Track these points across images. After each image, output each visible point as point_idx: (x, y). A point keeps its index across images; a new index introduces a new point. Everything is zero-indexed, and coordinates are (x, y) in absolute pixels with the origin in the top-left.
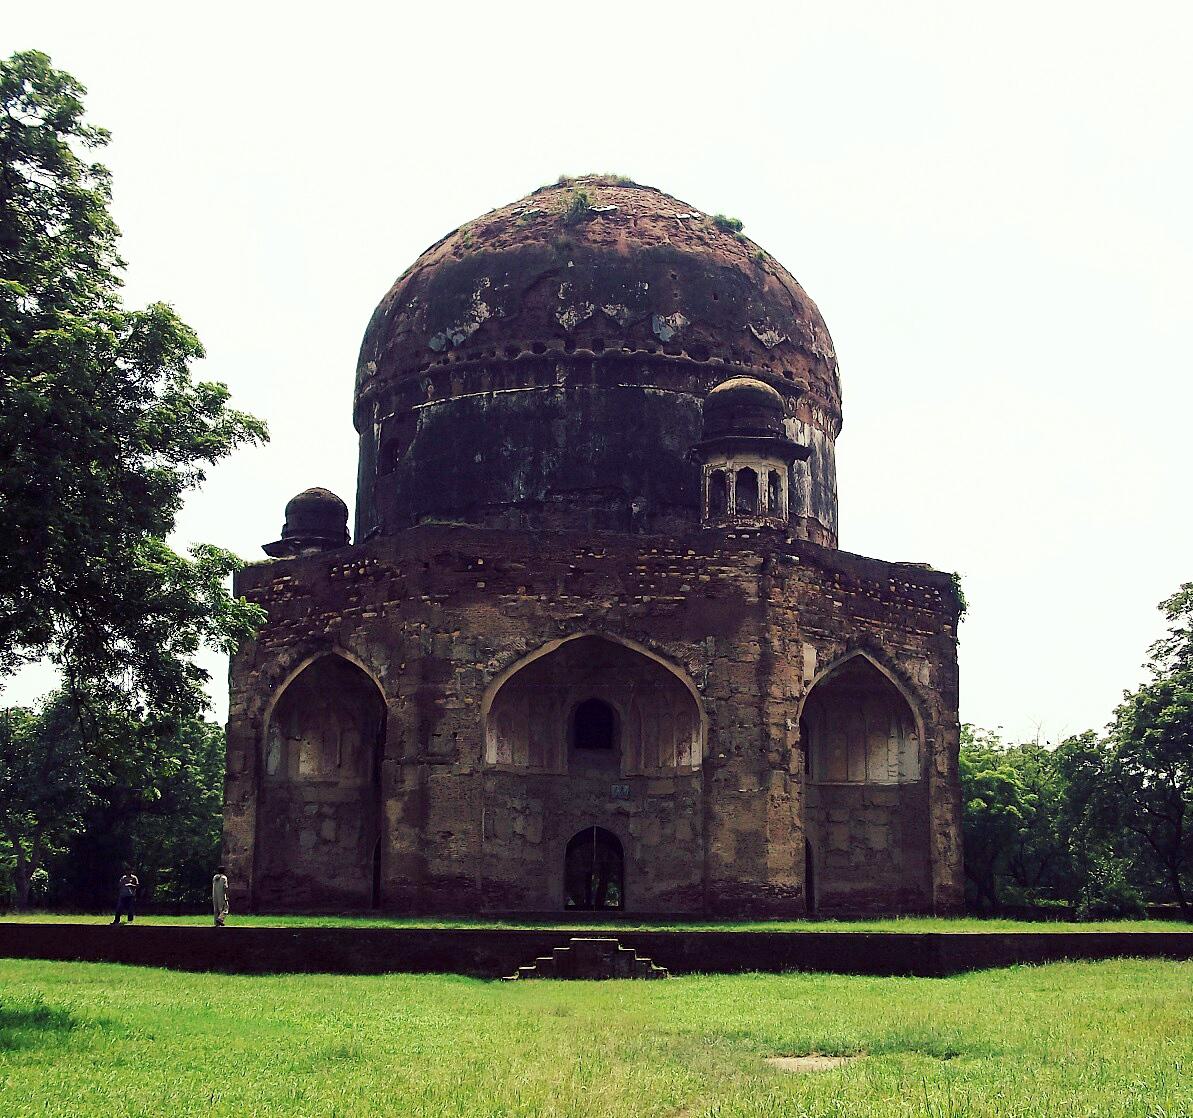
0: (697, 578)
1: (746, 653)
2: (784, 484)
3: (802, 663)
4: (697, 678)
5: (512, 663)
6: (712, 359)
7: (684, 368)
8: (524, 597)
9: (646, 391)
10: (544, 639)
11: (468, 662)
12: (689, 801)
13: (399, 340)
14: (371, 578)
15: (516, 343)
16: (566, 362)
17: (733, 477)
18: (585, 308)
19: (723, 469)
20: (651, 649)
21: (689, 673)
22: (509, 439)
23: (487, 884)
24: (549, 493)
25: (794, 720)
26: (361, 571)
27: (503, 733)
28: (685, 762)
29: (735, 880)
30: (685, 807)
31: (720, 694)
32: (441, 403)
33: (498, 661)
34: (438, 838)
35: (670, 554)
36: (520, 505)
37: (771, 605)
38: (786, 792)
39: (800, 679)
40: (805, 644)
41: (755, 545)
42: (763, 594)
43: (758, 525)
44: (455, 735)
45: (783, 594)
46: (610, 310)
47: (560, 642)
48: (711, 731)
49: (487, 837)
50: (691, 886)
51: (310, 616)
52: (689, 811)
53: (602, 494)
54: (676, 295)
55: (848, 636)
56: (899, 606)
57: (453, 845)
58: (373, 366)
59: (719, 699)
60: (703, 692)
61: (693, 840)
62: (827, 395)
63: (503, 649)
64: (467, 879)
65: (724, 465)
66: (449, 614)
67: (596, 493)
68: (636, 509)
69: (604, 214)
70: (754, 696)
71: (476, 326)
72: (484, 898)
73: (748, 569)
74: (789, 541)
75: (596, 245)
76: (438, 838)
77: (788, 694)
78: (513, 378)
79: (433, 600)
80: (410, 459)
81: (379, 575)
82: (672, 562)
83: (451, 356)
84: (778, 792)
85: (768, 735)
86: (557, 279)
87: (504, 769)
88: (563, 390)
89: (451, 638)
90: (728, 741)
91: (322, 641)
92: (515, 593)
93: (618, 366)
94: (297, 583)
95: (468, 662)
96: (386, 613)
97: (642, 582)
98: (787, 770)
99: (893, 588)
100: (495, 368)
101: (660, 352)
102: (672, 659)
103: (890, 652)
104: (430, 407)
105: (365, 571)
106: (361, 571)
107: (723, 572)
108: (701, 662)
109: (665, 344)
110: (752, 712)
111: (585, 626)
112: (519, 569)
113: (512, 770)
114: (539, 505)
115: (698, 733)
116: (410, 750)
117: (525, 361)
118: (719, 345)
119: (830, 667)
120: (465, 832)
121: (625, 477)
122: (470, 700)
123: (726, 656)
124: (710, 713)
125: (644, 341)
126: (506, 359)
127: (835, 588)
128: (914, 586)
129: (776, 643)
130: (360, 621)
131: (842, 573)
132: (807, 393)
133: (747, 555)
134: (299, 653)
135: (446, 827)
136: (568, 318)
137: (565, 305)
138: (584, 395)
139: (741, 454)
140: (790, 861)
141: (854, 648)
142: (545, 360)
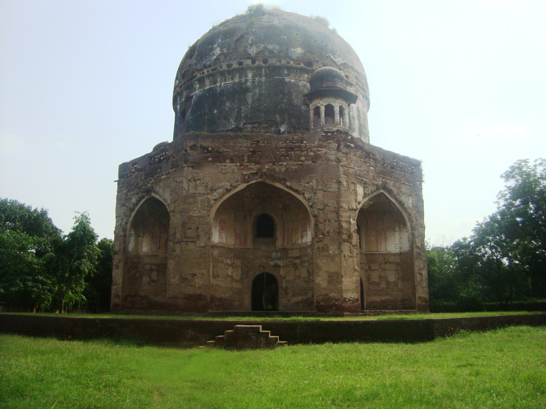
0: (308, 153)
1: (331, 187)
2: (346, 112)
3: (356, 194)
4: (308, 200)
5: (224, 194)
6: (314, 67)
7: (302, 71)
8: (229, 165)
9: (286, 80)
10: (238, 183)
11: (204, 194)
12: (306, 259)
13: (188, 68)
14: (165, 160)
15: (231, 62)
16: (251, 69)
17: (323, 109)
18: (259, 46)
19: (319, 105)
20: (287, 187)
21: (305, 198)
22: (228, 102)
23: (213, 298)
24: (245, 124)
25: (354, 220)
26: (162, 158)
27: (222, 229)
28: (304, 241)
29: (327, 295)
30: (304, 262)
31: (319, 207)
32: (201, 91)
33: (217, 194)
34: (190, 277)
35: (295, 143)
36: (232, 130)
37: (342, 166)
38: (351, 253)
39: (356, 201)
40: (358, 185)
41: (334, 138)
42: (339, 161)
43: (335, 129)
44: (198, 228)
45: (347, 161)
46: (270, 47)
47: (244, 185)
48: (316, 225)
49: (214, 277)
50: (308, 299)
51: (143, 181)
52: (307, 264)
53: (268, 124)
54: (298, 41)
55: (377, 183)
56: (398, 172)
57: (196, 280)
58: (177, 82)
59: (319, 209)
60: (311, 207)
61: (309, 277)
62: (363, 89)
63: (220, 188)
64: (202, 296)
65: (318, 103)
66: (196, 173)
67: (266, 123)
68: (282, 130)
69: (269, 14)
70: (335, 208)
71: (215, 57)
72: (213, 305)
73: (331, 149)
74: (349, 137)
75: (264, 23)
76: (190, 277)
77: (351, 207)
78: (230, 77)
79: (188, 167)
80: (189, 116)
81: (168, 158)
82: (296, 147)
83: (205, 71)
84: (347, 253)
85: (342, 227)
86: (248, 36)
88: (251, 80)
89: (196, 183)
90: (323, 229)
91: (148, 191)
92: (225, 162)
93: (275, 70)
94: (139, 167)
95: (204, 194)
96: (170, 175)
97: (283, 156)
98: (351, 243)
99: (395, 164)
100: (222, 74)
101: (292, 63)
102: (297, 191)
103: (395, 191)
104: (197, 92)
105: (163, 158)
106: (162, 158)
107: (319, 151)
108: (310, 192)
109: (294, 60)
110: (334, 215)
111: (257, 177)
112: (227, 152)
113: (226, 246)
114: (240, 130)
115: (310, 226)
116: (178, 236)
117: (234, 70)
118: (317, 62)
119: (370, 196)
120: (202, 274)
121: (277, 116)
122: (205, 212)
123: (321, 189)
124: (315, 216)
125: (285, 59)
126: (227, 69)
127: (371, 161)
128: (404, 164)
129: (345, 183)
130: (160, 181)
131: (373, 154)
132: (355, 85)
133: (330, 143)
134: (139, 197)
135: (195, 271)
136: (253, 51)
137: (251, 45)
138: (259, 82)
139: (326, 98)
140: (354, 286)
141: (380, 189)
142: (243, 69)
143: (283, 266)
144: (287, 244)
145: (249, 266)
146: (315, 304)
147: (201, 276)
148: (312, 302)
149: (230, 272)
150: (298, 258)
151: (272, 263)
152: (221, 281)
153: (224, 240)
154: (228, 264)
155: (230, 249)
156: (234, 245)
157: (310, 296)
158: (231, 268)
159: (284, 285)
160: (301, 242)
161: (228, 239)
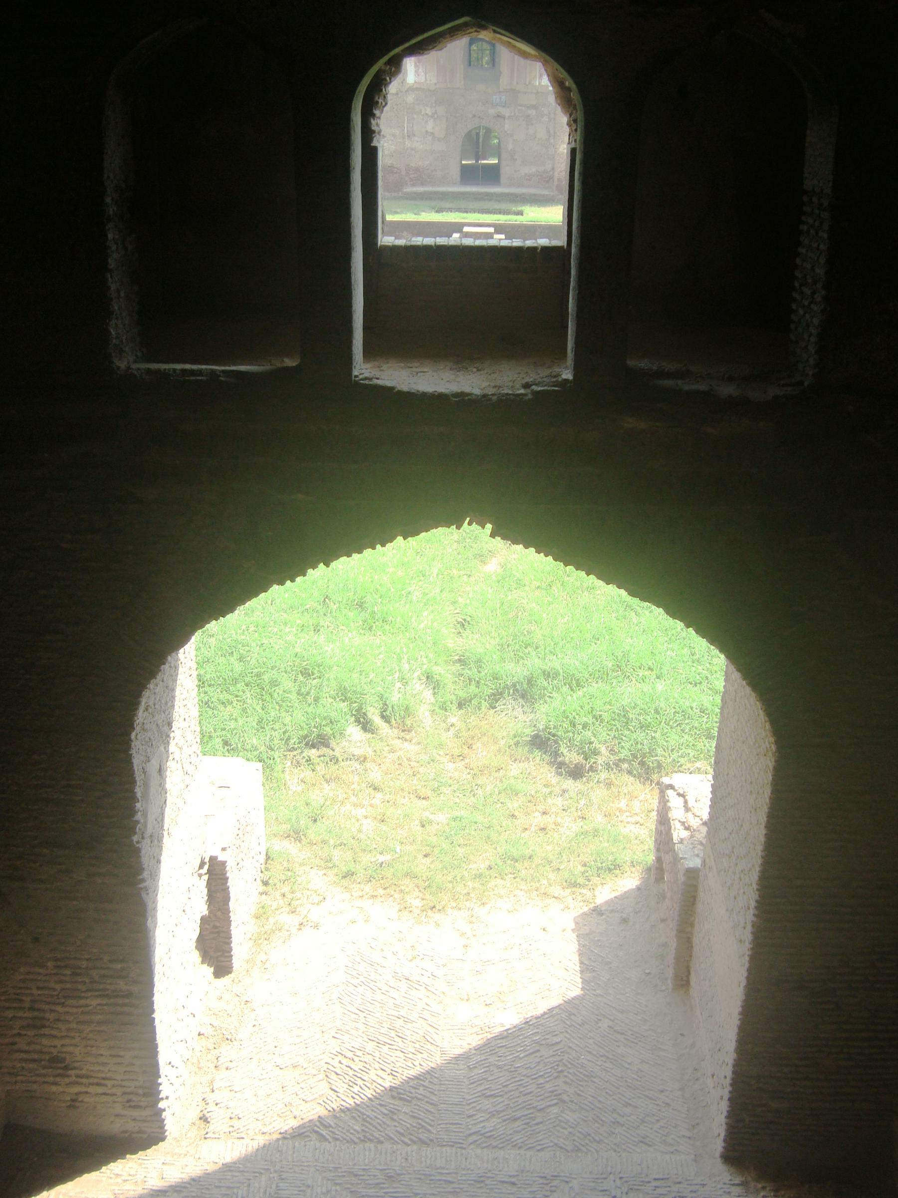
49: (409, 136)
52: (545, 119)
87: (418, 86)
120: (393, 135)
143: (509, 117)
144: (517, 83)
145: (458, 115)
146: (556, 183)
147: (393, 138)
148: (552, 178)
149: (429, 128)
150: (534, 107)
151: (492, 112)
152: (418, 142)
153: (423, 80)
154: (427, 114)
155: (429, 90)
156: (435, 84)
157: (548, 167)
158: (432, 120)
159: (510, 147)
160: (539, 83)
161: (428, 75)
